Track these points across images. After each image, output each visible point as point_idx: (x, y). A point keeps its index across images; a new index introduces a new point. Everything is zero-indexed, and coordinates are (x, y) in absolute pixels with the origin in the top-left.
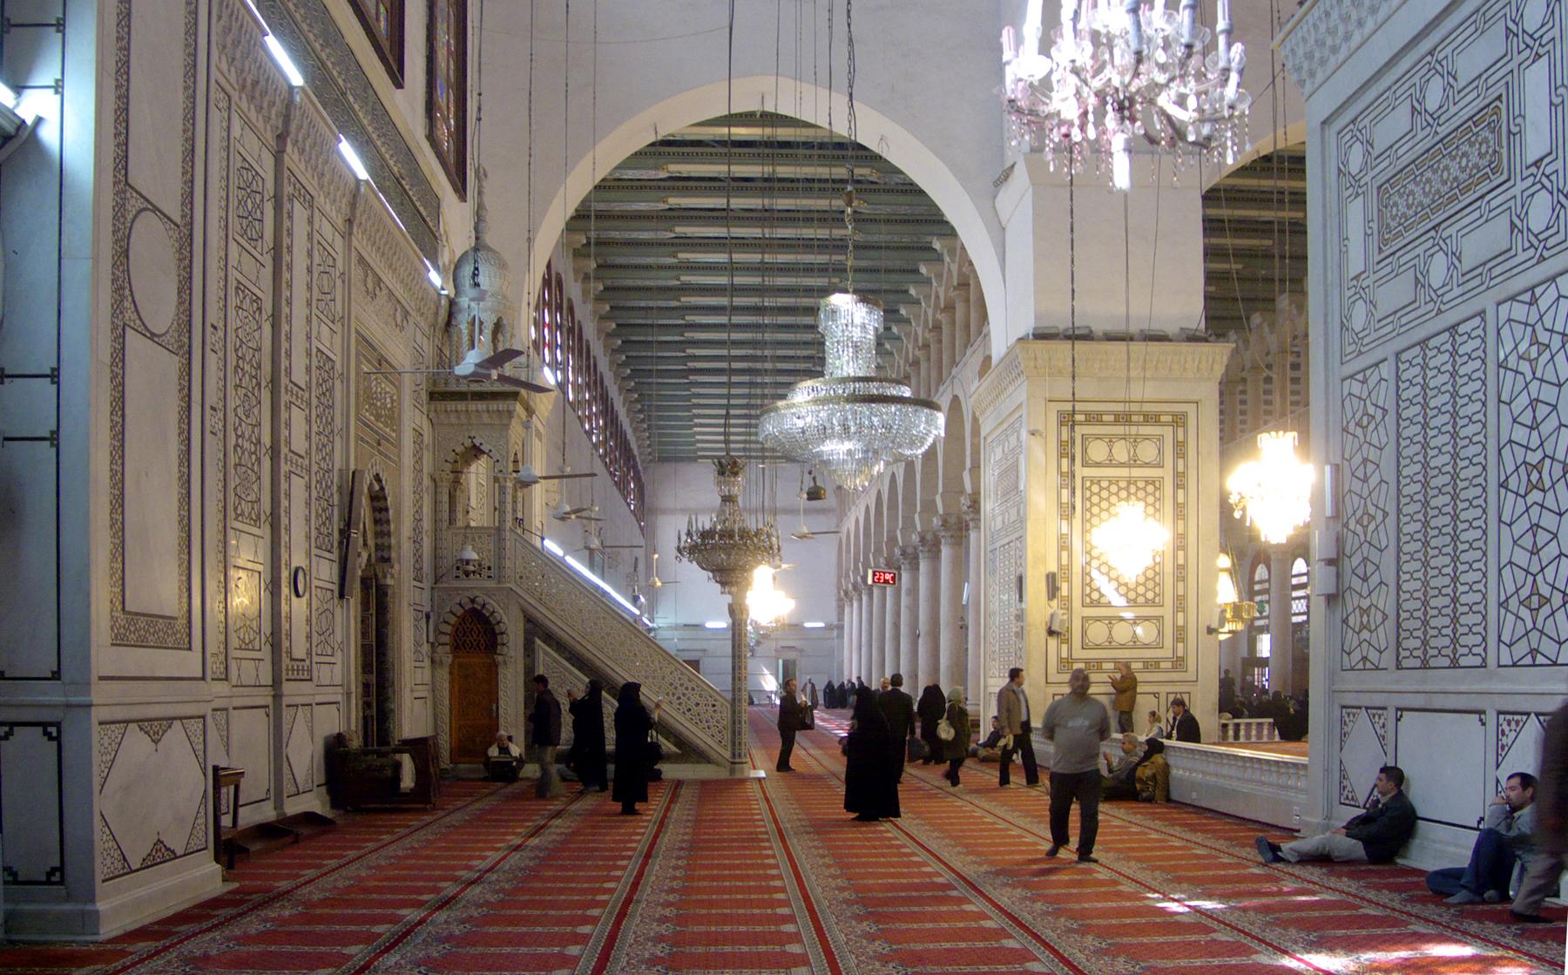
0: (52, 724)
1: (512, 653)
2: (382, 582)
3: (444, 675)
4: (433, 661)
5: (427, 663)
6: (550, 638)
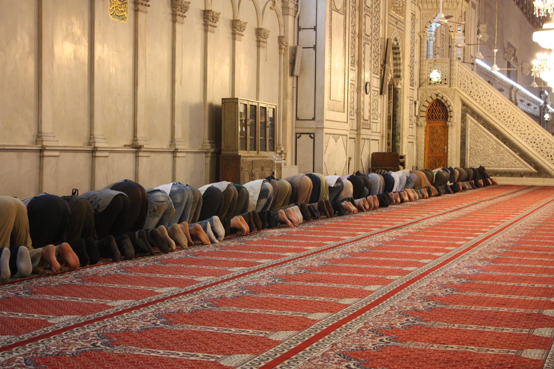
0: (312, 134)
1: (455, 121)
2: (396, 87)
3: (422, 131)
4: (417, 125)
5: (415, 125)
6: (474, 114)
